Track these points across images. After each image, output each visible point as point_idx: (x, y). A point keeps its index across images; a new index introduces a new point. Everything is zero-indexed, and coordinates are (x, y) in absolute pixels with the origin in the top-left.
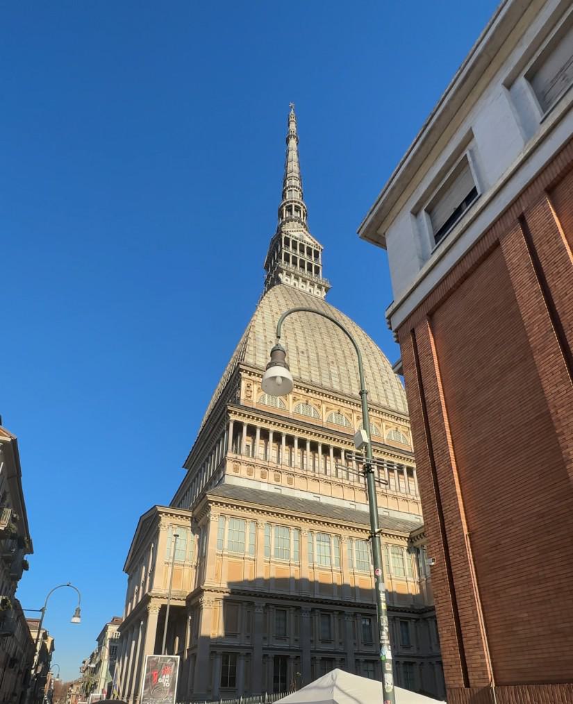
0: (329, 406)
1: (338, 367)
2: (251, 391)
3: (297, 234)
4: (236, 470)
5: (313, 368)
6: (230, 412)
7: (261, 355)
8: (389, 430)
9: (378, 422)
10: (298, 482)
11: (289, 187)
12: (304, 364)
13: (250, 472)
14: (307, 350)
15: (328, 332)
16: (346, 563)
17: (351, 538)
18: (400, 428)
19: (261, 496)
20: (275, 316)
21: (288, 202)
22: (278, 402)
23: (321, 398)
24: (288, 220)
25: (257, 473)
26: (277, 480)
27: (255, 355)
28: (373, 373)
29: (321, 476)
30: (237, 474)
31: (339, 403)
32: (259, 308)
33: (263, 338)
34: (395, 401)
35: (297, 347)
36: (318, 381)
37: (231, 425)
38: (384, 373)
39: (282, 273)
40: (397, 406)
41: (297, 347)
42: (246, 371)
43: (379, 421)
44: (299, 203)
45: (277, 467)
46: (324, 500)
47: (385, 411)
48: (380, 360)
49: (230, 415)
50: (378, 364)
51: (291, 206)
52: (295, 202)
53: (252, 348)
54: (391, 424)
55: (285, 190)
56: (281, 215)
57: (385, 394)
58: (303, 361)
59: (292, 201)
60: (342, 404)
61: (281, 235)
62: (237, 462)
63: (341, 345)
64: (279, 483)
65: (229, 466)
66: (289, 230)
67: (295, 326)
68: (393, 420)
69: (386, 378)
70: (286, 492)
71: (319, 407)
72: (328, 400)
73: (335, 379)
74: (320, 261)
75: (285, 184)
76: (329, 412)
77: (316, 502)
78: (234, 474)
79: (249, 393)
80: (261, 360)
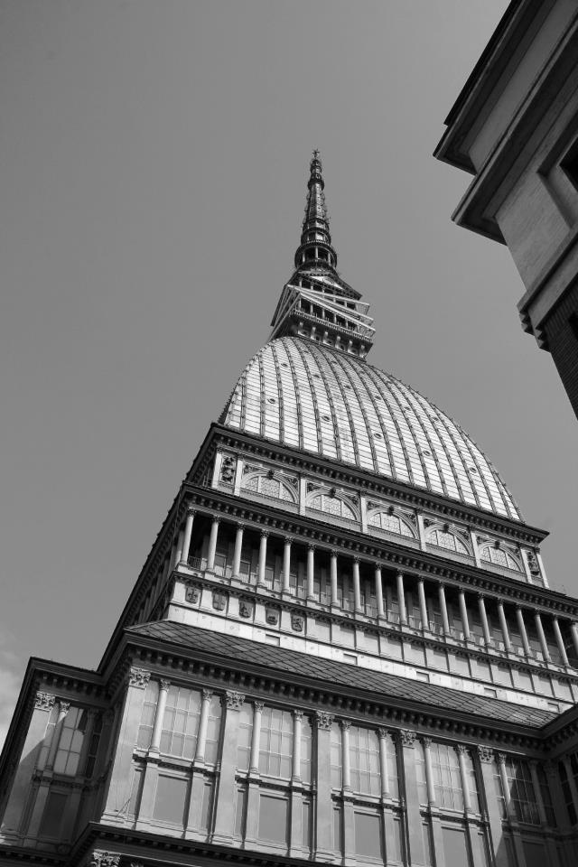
1: (387, 443)
3: (320, 279)
10: (313, 628)
14: (334, 416)
15: (370, 395)
18: (503, 543)
20: (282, 368)
25: (234, 606)
26: (271, 620)
28: (448, 456)
33: (259, 395)
34: (491, 499)
35: (316, 411)
36: (354, 462)
37: (191, 520)
38: (466, 455)
40: (492, 505)
41: (316, 411)
42: (226, 439)
43: (464, 530)
46: (363, 662)
50: (455, 443)
51: (314, 250)
53: (239, 408)
54: (487, 537)
57: (473, 488)
63: (392, 414)
64: (276, 627)
70: (287, 643)
73: (383, 461)
79: (229, 472)
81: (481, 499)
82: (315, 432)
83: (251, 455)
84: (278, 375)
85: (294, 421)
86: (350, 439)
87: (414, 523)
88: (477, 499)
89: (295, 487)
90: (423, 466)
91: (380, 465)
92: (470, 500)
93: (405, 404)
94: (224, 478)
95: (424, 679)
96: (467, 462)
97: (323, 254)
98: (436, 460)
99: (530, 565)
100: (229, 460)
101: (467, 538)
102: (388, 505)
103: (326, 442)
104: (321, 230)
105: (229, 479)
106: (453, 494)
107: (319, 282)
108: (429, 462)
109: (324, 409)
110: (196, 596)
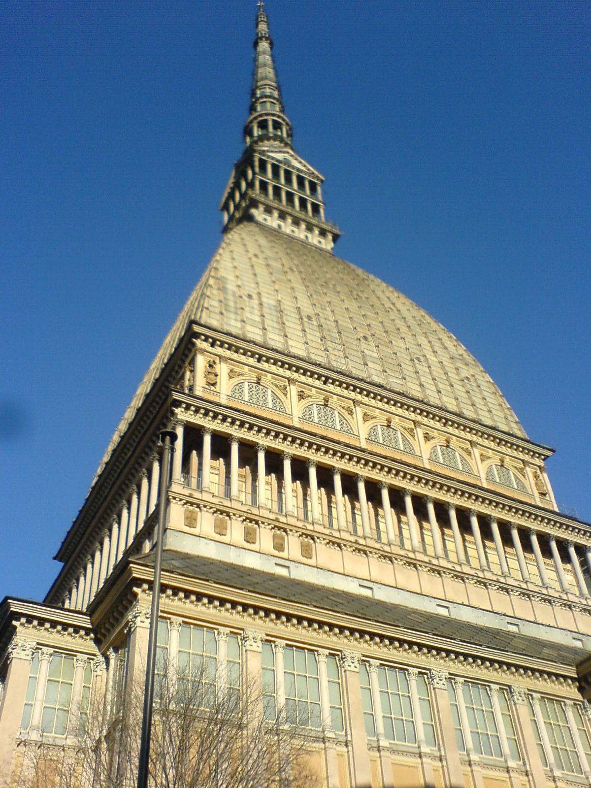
0: (369, 412)
2: (216, 375)
4: (191, 521)
5: (329, 344)
6: (177, 403)
7: (233, 316)
8: (488, 462)
9: (465, 446)
10: (324, 554)
11: (261, 97)
12: (314, 336)
13: (221, 529)
16: (450, 737)
17: (452, 677)
18: (507, 459)
19: (249, 578)
21: (261, 115)
22: (270, 398)
23: (353, 395)
24: (261, 138)
26: (279, 547)
27: (221, 313)
29: (371, 543)
30: (191, 530)
31: (386, 407)
32: (224, 245)
33: (236, 289)
35: (298, 309)
37: (180, 431)
39: (256, 207)
41: (298, 309)
44: (279, 117)
45: (277, 520)
46: (382, 595)
47: (472, 425)
48: (450, 344)
49: (178, 411)
50: (446, 348)
51: (266, 121)
52: (273, 115)
53: (216, 304)
54: (490, 453)
55: (255, 102)
56: (248, 131)
58: (311, 332)
59: (267, 114)
60: (393, 409)
61: (253, 156)
62: (192, 504)
64: (284, 554)
65: (176, 514)
66: (266, 149)
67: (289, 277)
68: (493, 445)
69: (464, 373)
71: (351, 413)
72: (366, 400)
74: (320, 197)
75: (253, 94)
76: (370, 424)
77: (366, 598)
78: (187, 529)
79: (212, 376)
80: (233, 322)
81: (480, 412)
82: (301, 334)
83: (235, 356)
84: (252, 266)
85: (275, 319)
86: (338, 341)
87: (413, 436)
88: (476, 412)
89: (285, 395)
90: (417, 372)
91: (373, 372)
92: (469, 413)
93: (388, 305)
94: (209, 384)
95: (443, 612)
96: (460, 369)
97: (277, 126)
98: (429, 367)
99: (536, 484)
100: (212, 363)
101: (469, 454)
102: (386, 416)
103: (314, 345)
104: (274, 98)
105: (214, 384)
106: (452, 406)
107: (278, 161)
108: (422, 368)
109: (307, 309)
110: (195, 520)
